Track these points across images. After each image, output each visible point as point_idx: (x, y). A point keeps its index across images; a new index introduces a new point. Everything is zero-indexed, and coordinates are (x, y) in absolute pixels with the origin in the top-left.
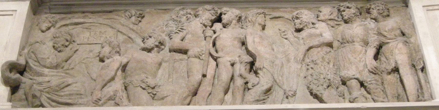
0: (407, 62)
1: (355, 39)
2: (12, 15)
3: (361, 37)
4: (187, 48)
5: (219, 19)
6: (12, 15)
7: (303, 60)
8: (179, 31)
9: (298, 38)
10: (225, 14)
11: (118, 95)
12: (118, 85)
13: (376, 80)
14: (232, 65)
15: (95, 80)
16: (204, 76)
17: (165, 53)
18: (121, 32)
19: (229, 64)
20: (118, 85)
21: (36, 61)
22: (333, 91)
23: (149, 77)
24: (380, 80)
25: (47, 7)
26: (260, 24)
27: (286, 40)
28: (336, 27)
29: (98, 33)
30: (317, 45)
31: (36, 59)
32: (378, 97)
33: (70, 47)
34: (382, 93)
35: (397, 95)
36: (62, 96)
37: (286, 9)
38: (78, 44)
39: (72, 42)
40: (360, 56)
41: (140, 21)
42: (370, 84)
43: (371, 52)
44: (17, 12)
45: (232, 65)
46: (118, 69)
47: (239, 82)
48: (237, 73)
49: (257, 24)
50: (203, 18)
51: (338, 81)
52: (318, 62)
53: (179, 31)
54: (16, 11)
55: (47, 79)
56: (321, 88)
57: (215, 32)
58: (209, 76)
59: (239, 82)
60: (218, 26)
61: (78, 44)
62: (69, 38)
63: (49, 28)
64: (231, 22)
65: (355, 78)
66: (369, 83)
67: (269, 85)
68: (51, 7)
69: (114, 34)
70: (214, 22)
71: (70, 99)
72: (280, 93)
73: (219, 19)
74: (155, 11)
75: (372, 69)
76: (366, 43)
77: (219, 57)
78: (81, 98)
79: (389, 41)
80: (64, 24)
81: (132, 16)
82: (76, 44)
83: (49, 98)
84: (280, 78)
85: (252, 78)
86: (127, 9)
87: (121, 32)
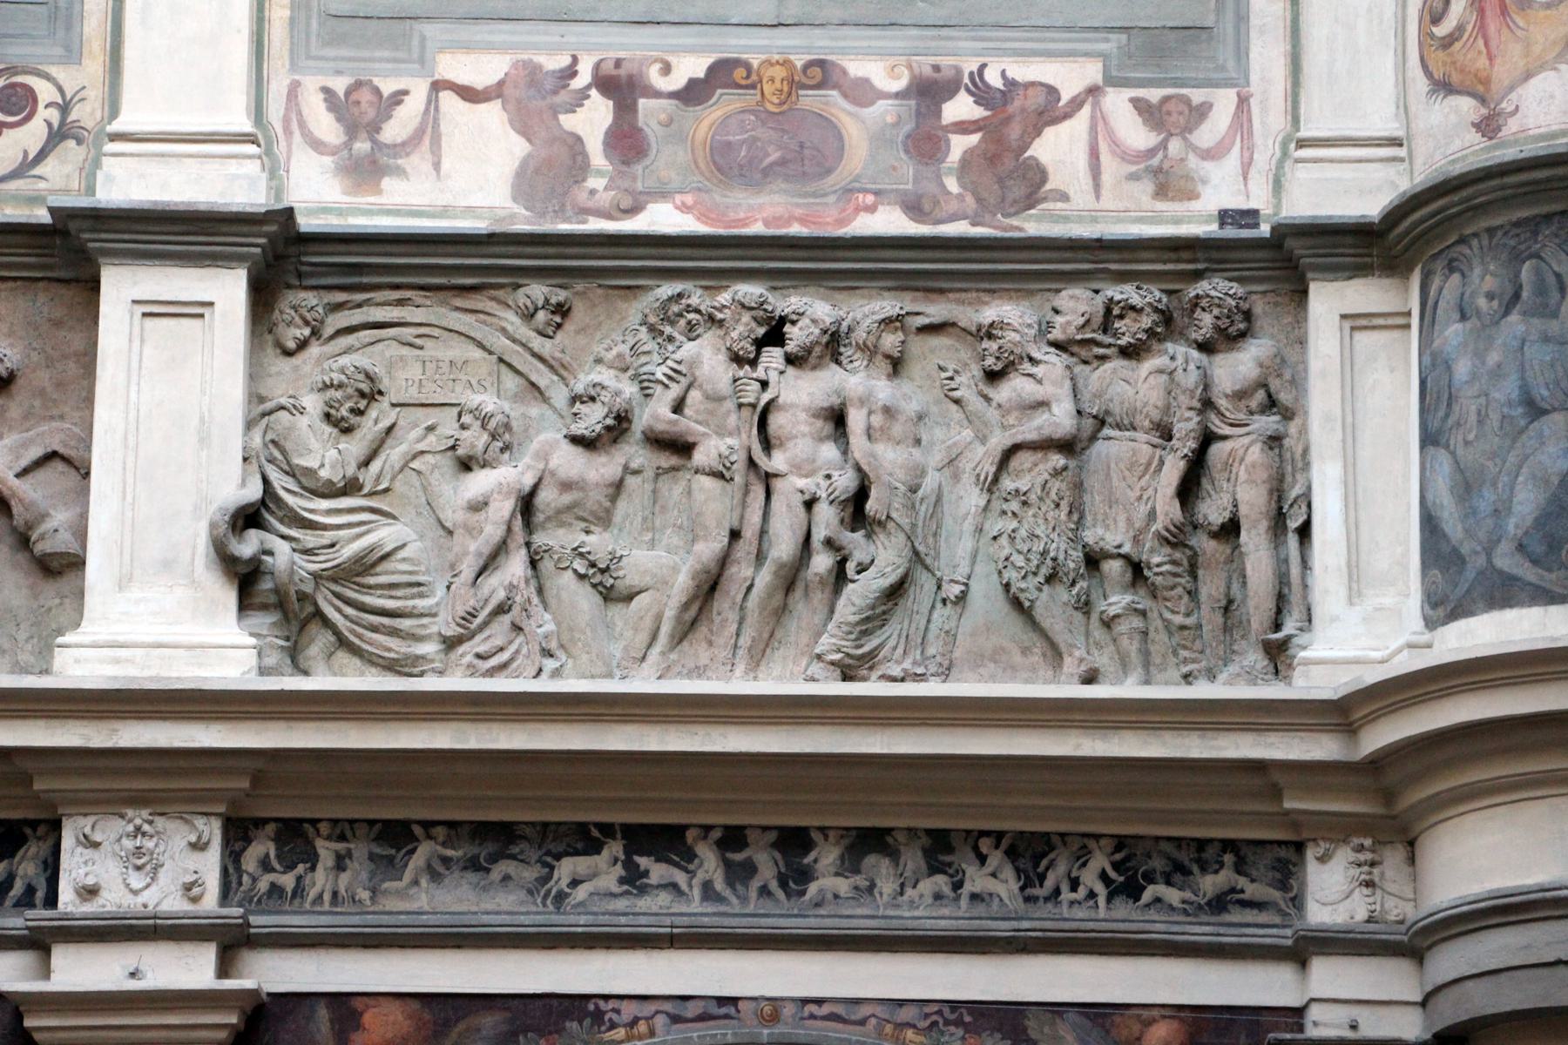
0: (1264, 509)
1: (1137, 422)
2: (202, 316)
3: (1156, 415)
4: (691, 439)
5: (774, 334)
6: (202, 316)
7: (996, 480)
8: (670, 378)
9: (987, 399)
10: (793, 323)
11: (518, 599)
12: (515, 566)
13: (1174, 562)
14: (809, 504)
15: (450, 533)
16: (735, 535)
17: (633, 452)
18: (510, 366)
19: (798, 500)
20: (515, 566)
21: (287, 473)
22: (1063, 594)
23: (592, 528)
24: (1185, 562)
25: (291, 268)
26: (888, 357)
27: (954, 407)
28: (1095, 364)
29: (445, 367)
30: (1033, 442)
31: (286, 468)
32: (1173, 612)
33: (373, 413)
34: (1186, 598)
35: (1224, 603)
36: (370, 587)
37: (963, 295)
38: (394, 405)
39: (372, 394)
40: (1143, 482)
41: (559, 326)
42: (1157, 574)
43: (1173, 469)
44: (216, 307)
45: (809, 504)
46: (513, 515)
47: (822, 562)
48: (819, 535)
49: (879, 357)
50: (735, 335)
51: (1073, 560)
52: (1033, 497)
53: (670, 378)
54: (211, 304)
55: (329, 536)
56: (1033, 582)
57: (764, 384)
58: (750, 533)
59: (822, 562)
60: (773, 357)
61: (394, 405)
62: (365, 387)
63: (303, 345)
64: (810, 352)
65: (1120, 555)
66: (1157, 570)
67: (900, 571)
68: (305, 268)
69: (490, 374)
70: (760, 344)
71: (391, 597)
72: (926, 587)
73: (774, 334)
74: (600, 291)
75: (1167, 530)
76: (1165, 432)
77: (776, 476)
78: (421, 596)
79: (1227, 430)
80: (345, 324)
81: (536, 310)
82: (384, 403)
83: (338, 596)
84: (931, 540)
85: (855, 541)
86: (521, 281)
87: (510, 366)
